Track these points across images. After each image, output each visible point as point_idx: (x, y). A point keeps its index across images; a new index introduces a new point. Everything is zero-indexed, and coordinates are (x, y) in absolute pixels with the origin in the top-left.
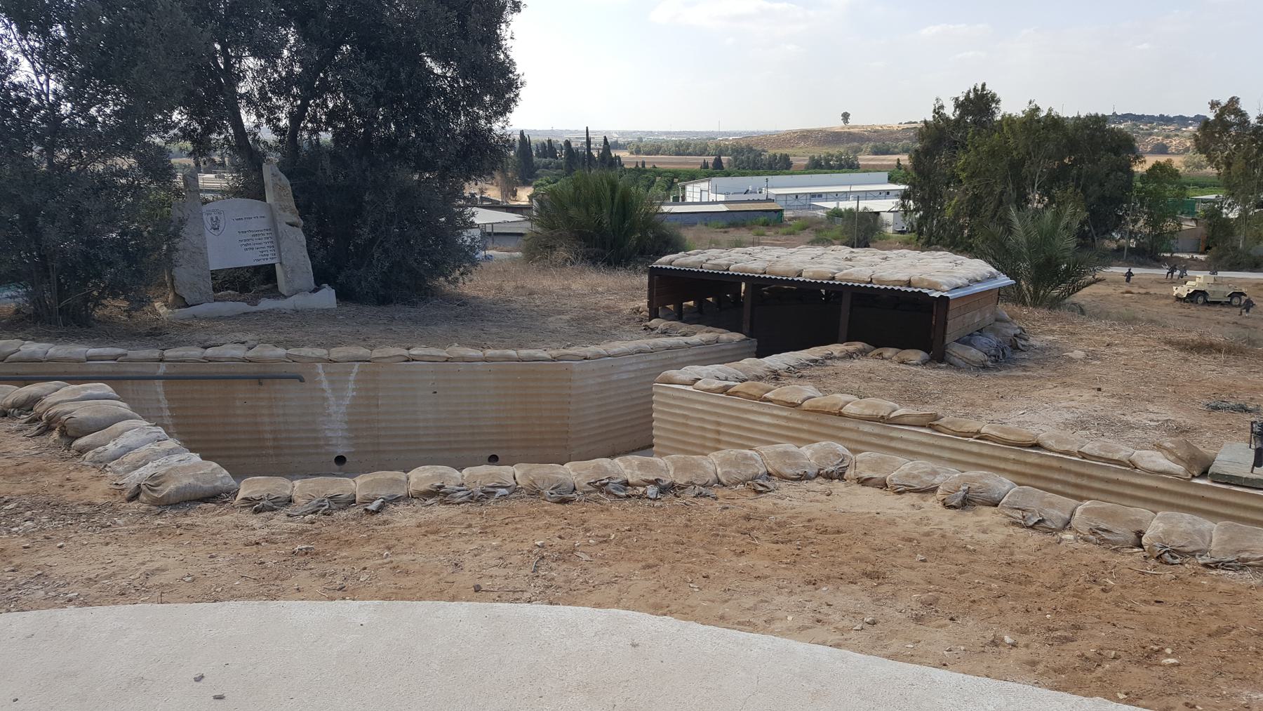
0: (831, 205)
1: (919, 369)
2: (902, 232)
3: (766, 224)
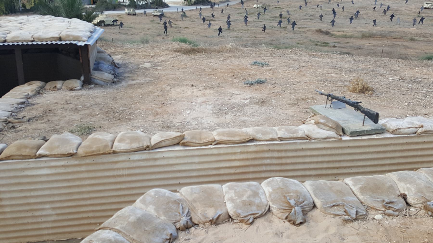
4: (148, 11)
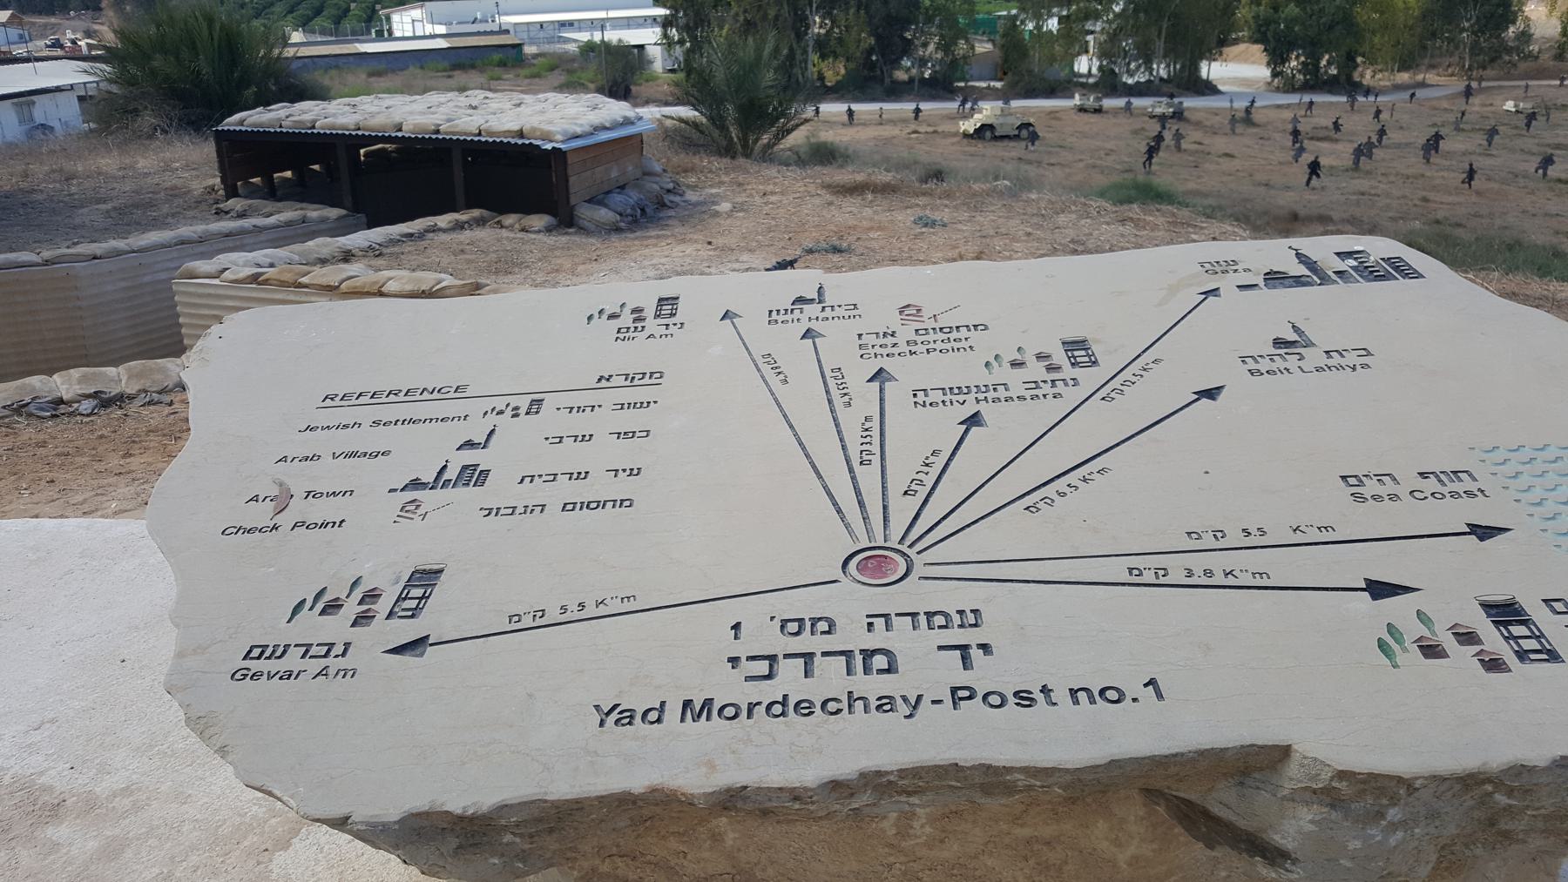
0: (584, 37)
1: (540, 236)
2: (672, 71)
3: (502, 64)
4: (1137, 102)
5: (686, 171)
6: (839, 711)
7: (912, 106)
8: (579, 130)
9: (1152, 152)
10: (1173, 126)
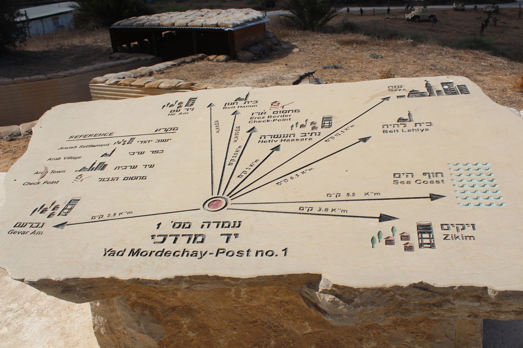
1: (223, 63)
5: (284, 36)
6: (178, 255)
7: (386, 8)
8: (239, 23)
9: (483, 27)
10: (494, 16)
